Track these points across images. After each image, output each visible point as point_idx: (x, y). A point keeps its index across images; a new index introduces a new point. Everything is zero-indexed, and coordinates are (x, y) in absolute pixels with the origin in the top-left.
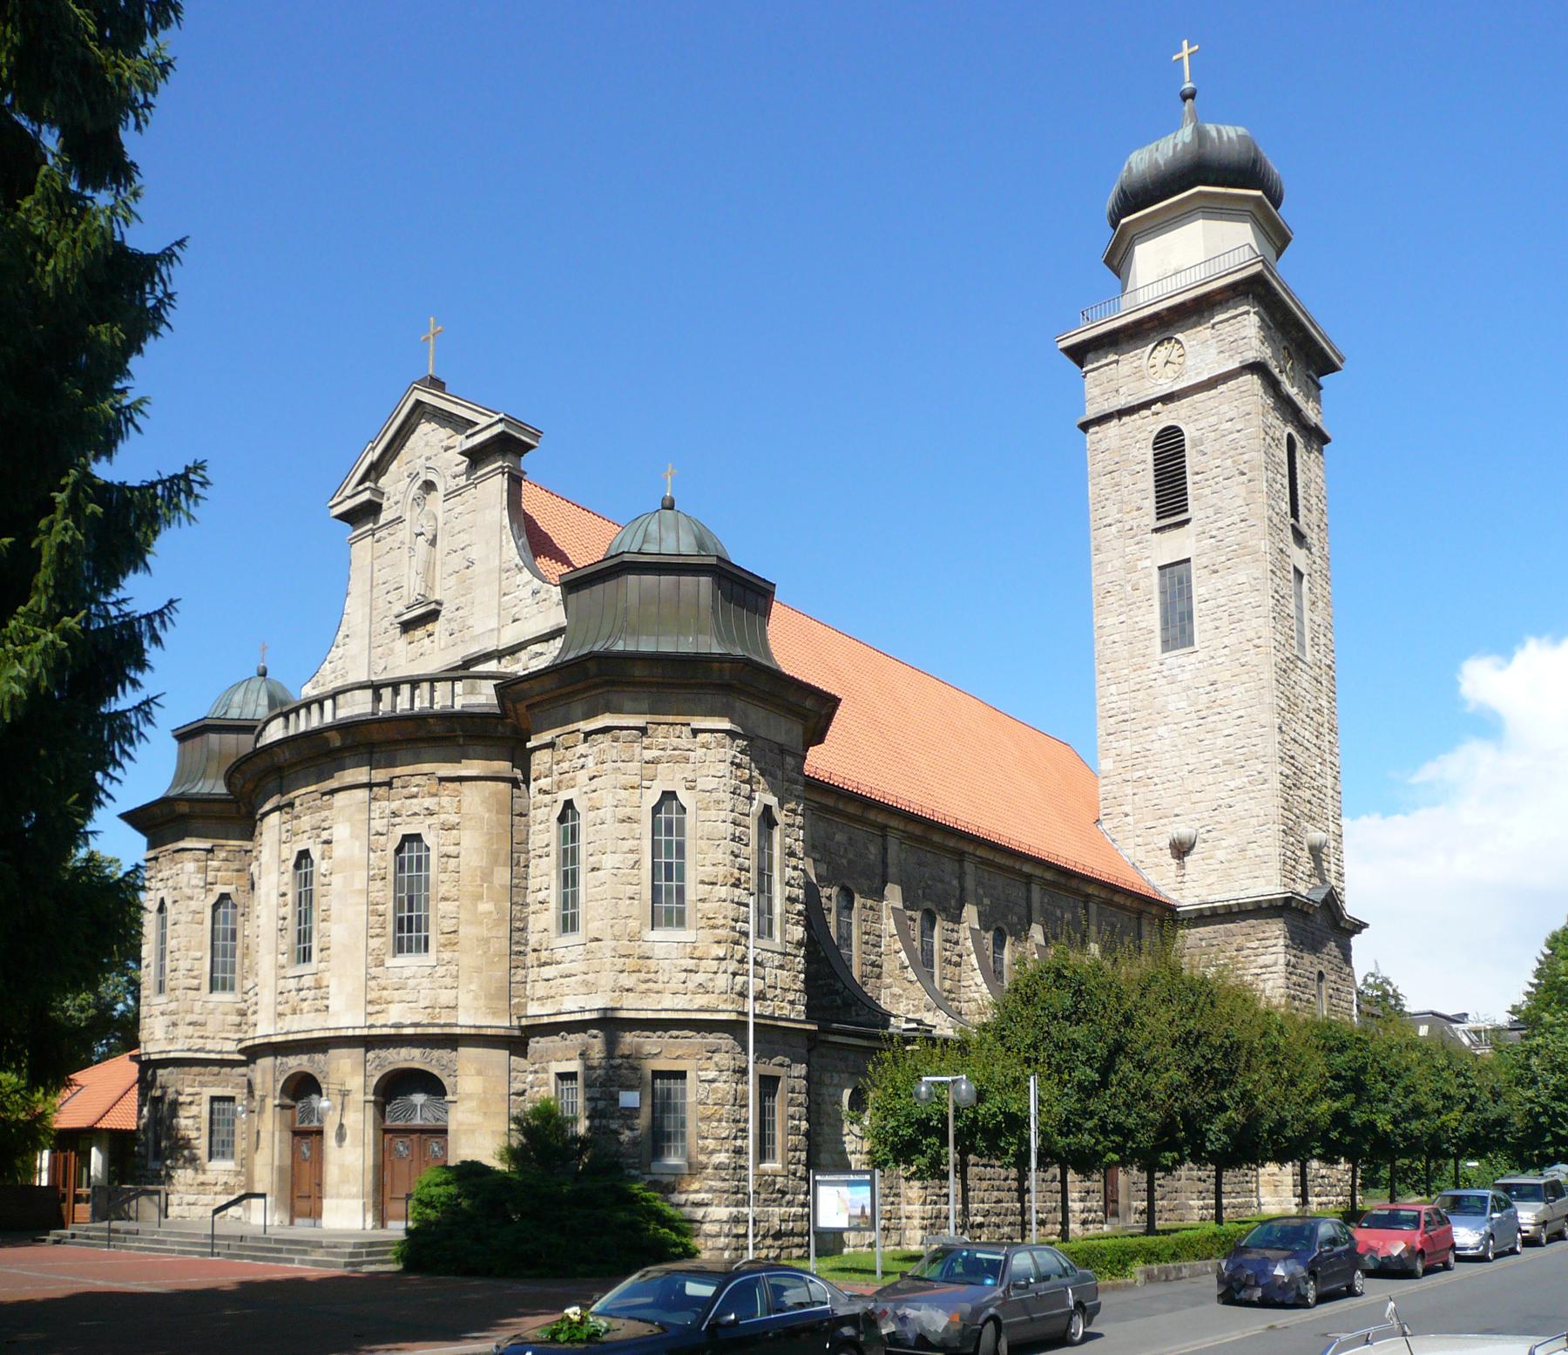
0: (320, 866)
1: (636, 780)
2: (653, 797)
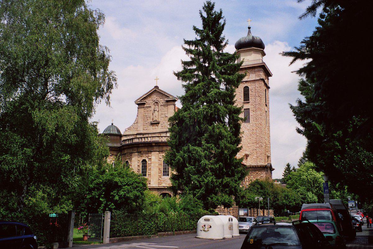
0: (148, 162)
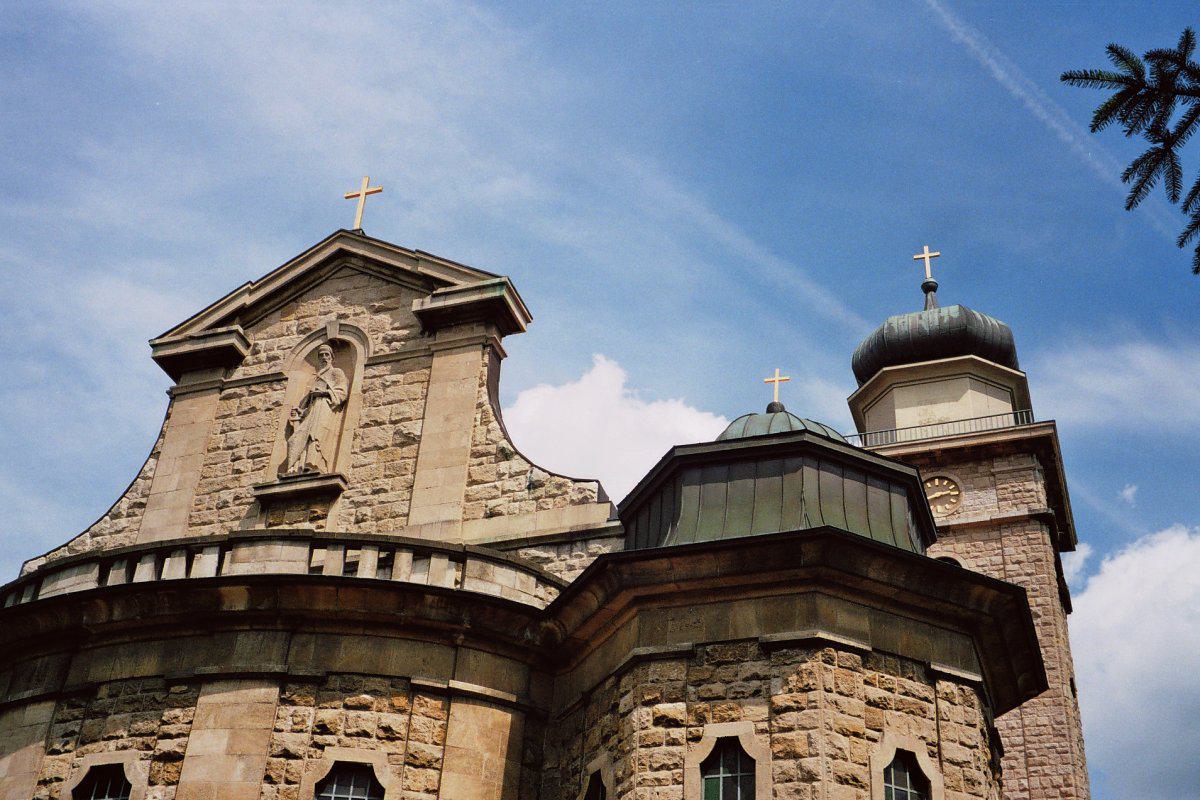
1: (860, 725)
2: (883, 756)
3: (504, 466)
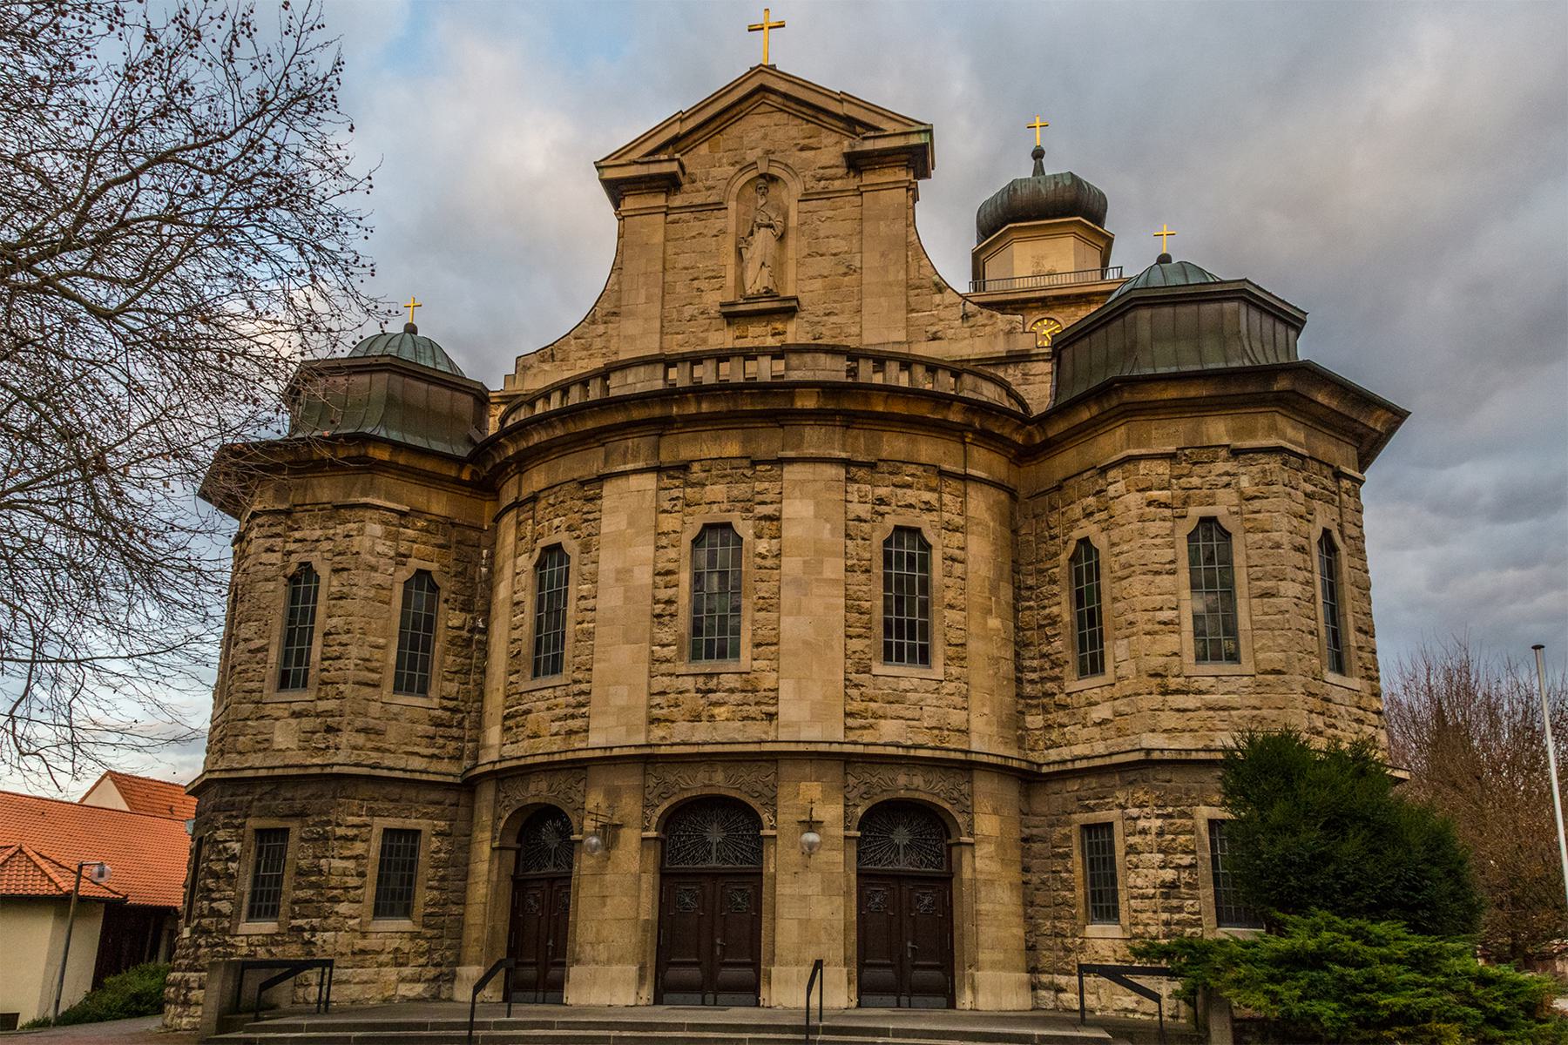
1: (1303, 510)
2: (1316, 534)
3: (937, 298)
